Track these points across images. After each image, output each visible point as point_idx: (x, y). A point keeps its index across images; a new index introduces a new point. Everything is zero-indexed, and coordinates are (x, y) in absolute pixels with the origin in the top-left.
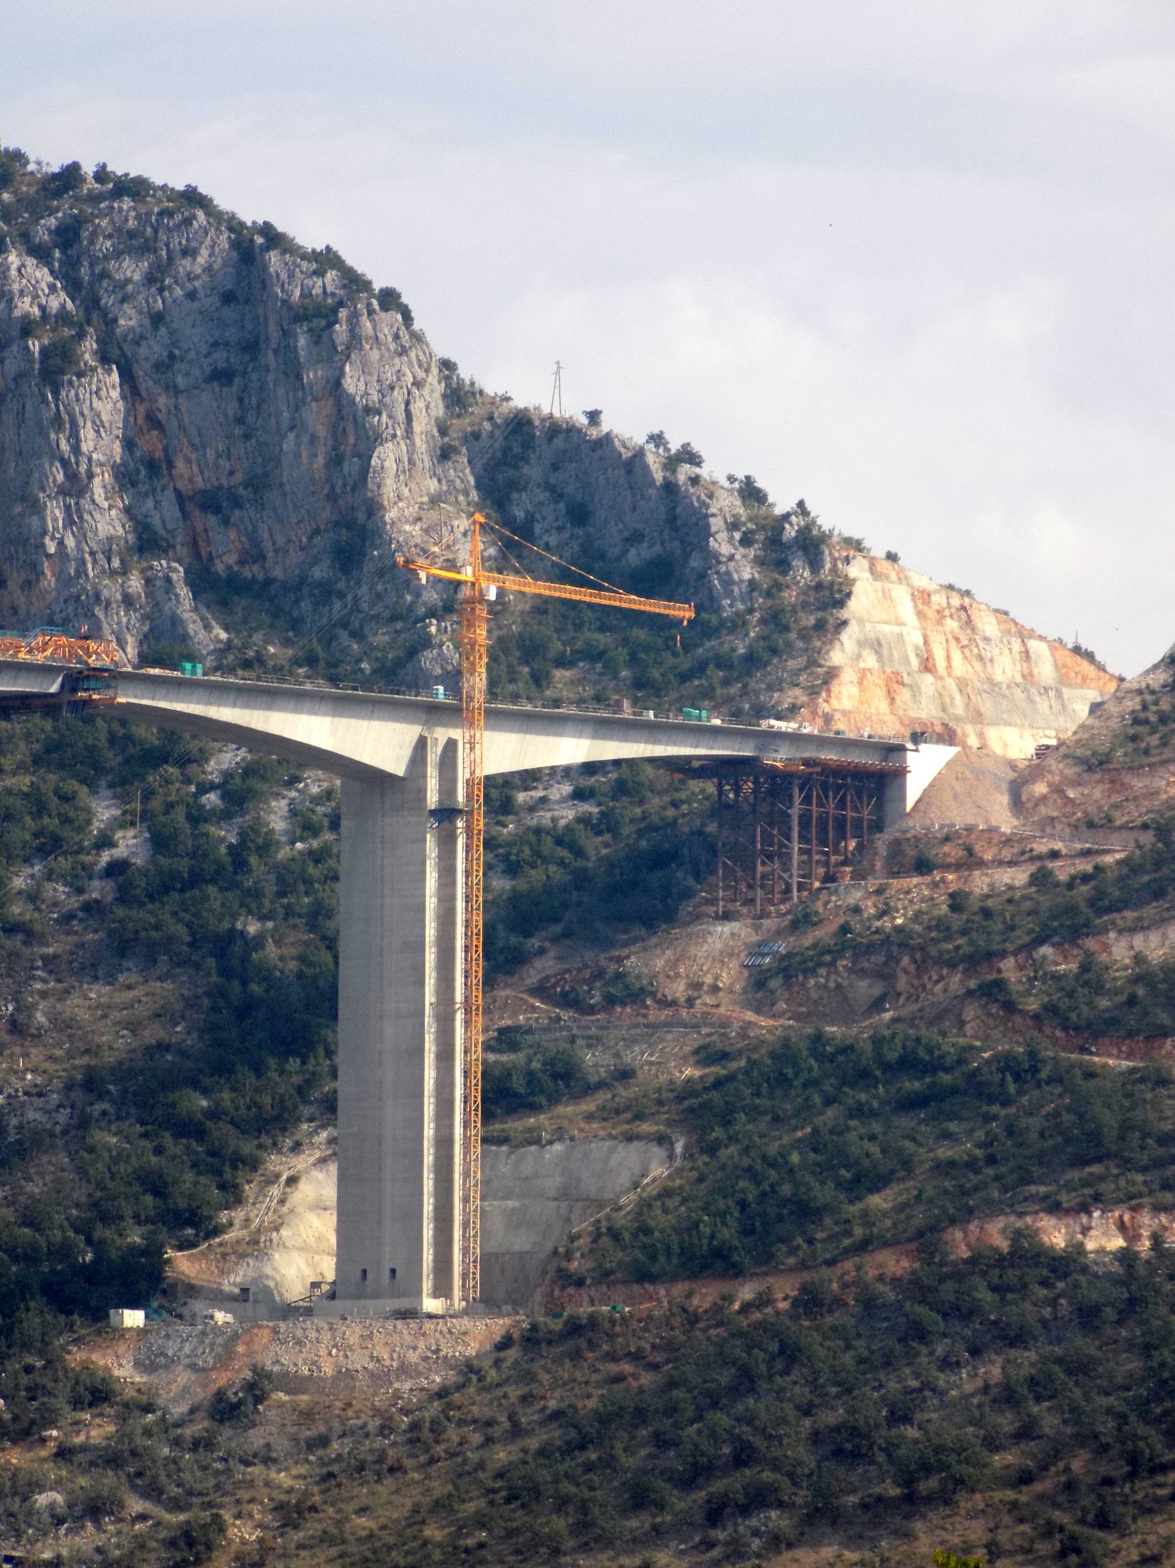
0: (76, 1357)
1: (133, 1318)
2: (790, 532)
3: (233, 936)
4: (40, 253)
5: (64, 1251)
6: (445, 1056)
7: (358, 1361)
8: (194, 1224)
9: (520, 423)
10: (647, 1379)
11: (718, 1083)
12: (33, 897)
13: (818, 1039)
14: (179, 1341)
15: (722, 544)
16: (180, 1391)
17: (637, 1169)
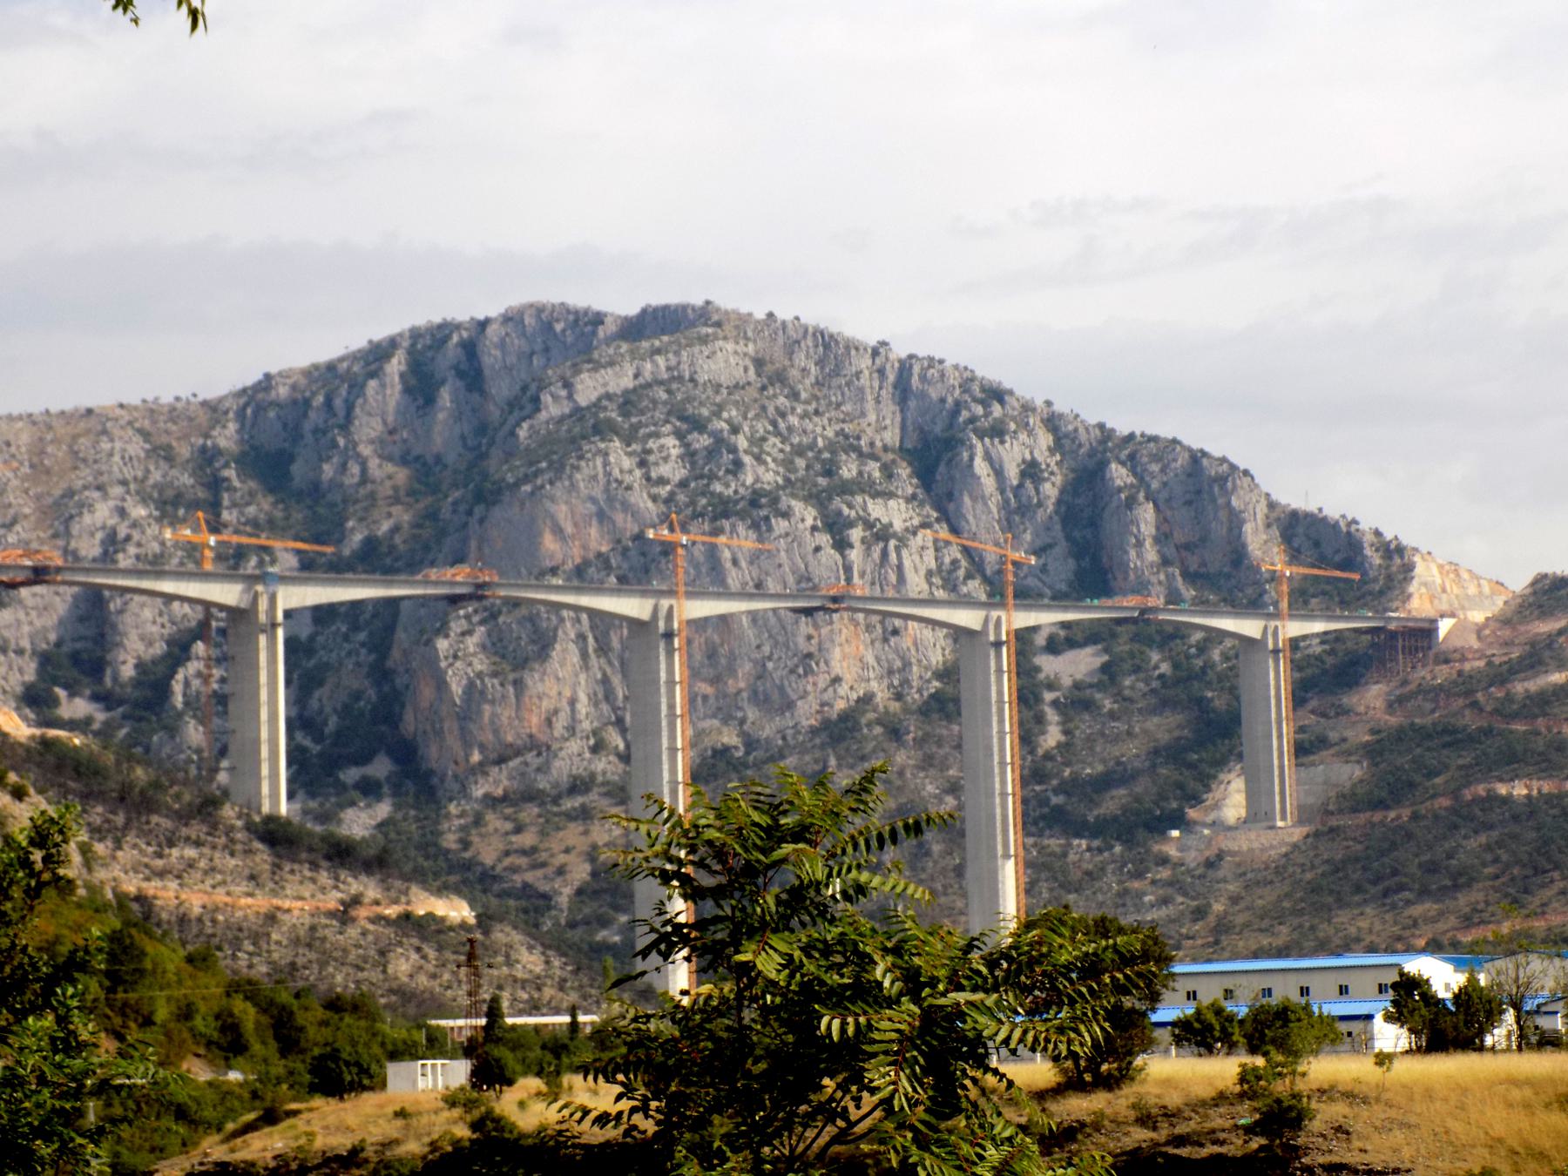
0: (1156, 848)
1: (1175, 833)
2: (1392, 546)
4: (1123, 464)
5: (1150, 811)
6: (1280, 737)
7: (1256, 845)
8: (1195, 799)
9: (1294, 515)
10: (1359, 847)
11: (1378, 741)
12: (1132, 688)
13: (1412, 724)
14: (1192, 841)
15: (1368, 552)
16: (1193, 858)
17: (1350, 773)
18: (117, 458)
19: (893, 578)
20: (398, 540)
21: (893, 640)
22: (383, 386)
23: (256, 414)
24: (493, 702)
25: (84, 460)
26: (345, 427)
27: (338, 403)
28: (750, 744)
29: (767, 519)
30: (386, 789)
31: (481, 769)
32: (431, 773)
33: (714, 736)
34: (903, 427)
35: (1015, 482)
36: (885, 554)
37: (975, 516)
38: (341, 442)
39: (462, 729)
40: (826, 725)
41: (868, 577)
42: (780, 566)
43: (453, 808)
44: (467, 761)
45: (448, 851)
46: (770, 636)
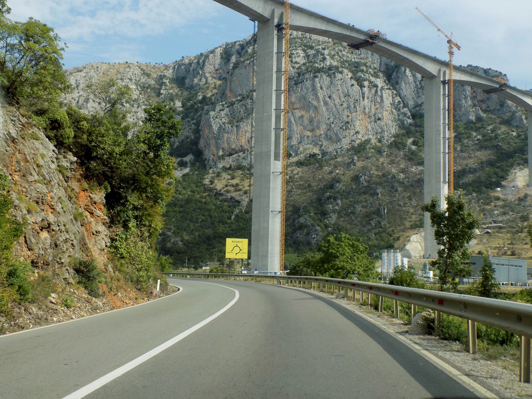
0: (492, 194)
1: (499, 189)
3: (498, 145)
5: (485, 182)
8: (504, 178)
18: (131, 73)
19: (379, 100)
20: (213, 98)
21: (378, 122)
22: (215, 56)
23: (178, 67)
24: (228, 133)
25: (120, 73)
26: (202, 68)
27: (201, 61)
28: (324, 154)
29: (334, 73)
30: (189, 165)
31: (222, 157)
32: (206, 159)
33: (310, 150)
34: (380, 64)
35: (420, 79)
36: (376, 91)
37: (406, 89)
38: (201, 72)
39: (216, 142)
40: (353, 148)
41: (370, 99)
42: (338, 90)
43: (211, 171)
44: (217, 154)
45: (205, 185)
46: (333, 115)
